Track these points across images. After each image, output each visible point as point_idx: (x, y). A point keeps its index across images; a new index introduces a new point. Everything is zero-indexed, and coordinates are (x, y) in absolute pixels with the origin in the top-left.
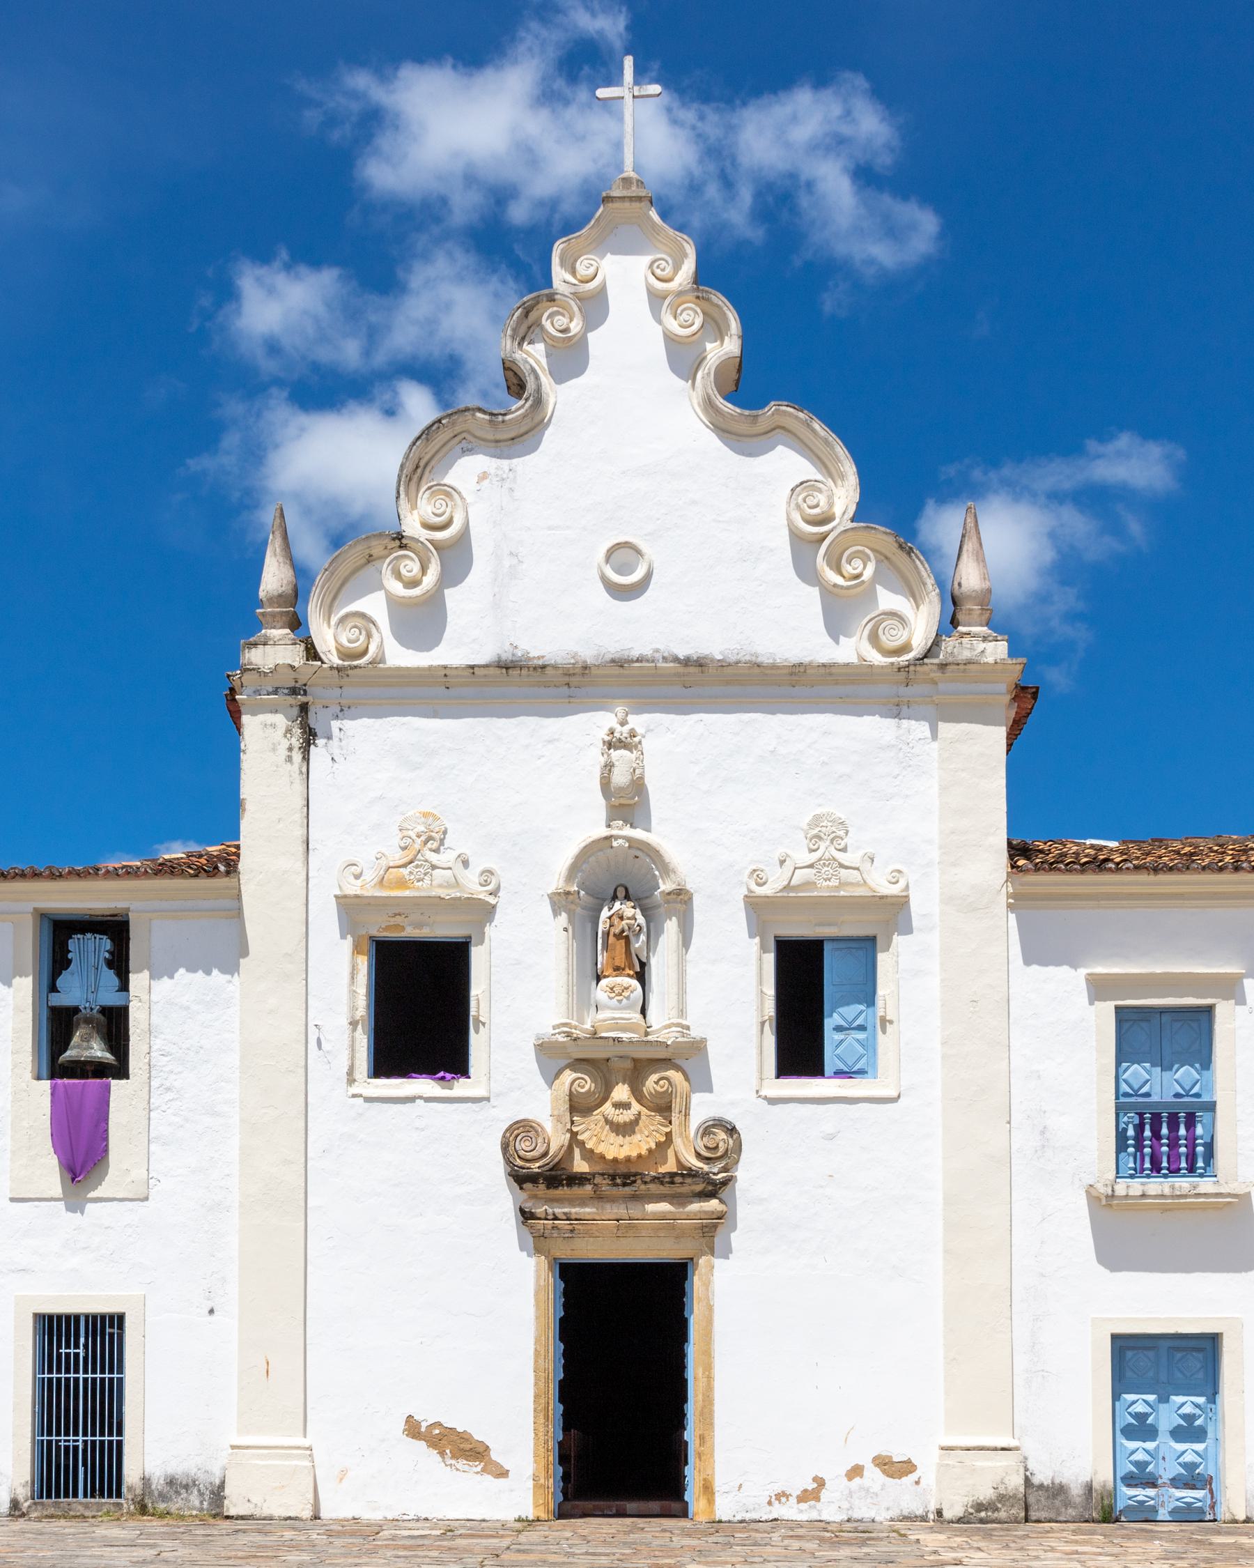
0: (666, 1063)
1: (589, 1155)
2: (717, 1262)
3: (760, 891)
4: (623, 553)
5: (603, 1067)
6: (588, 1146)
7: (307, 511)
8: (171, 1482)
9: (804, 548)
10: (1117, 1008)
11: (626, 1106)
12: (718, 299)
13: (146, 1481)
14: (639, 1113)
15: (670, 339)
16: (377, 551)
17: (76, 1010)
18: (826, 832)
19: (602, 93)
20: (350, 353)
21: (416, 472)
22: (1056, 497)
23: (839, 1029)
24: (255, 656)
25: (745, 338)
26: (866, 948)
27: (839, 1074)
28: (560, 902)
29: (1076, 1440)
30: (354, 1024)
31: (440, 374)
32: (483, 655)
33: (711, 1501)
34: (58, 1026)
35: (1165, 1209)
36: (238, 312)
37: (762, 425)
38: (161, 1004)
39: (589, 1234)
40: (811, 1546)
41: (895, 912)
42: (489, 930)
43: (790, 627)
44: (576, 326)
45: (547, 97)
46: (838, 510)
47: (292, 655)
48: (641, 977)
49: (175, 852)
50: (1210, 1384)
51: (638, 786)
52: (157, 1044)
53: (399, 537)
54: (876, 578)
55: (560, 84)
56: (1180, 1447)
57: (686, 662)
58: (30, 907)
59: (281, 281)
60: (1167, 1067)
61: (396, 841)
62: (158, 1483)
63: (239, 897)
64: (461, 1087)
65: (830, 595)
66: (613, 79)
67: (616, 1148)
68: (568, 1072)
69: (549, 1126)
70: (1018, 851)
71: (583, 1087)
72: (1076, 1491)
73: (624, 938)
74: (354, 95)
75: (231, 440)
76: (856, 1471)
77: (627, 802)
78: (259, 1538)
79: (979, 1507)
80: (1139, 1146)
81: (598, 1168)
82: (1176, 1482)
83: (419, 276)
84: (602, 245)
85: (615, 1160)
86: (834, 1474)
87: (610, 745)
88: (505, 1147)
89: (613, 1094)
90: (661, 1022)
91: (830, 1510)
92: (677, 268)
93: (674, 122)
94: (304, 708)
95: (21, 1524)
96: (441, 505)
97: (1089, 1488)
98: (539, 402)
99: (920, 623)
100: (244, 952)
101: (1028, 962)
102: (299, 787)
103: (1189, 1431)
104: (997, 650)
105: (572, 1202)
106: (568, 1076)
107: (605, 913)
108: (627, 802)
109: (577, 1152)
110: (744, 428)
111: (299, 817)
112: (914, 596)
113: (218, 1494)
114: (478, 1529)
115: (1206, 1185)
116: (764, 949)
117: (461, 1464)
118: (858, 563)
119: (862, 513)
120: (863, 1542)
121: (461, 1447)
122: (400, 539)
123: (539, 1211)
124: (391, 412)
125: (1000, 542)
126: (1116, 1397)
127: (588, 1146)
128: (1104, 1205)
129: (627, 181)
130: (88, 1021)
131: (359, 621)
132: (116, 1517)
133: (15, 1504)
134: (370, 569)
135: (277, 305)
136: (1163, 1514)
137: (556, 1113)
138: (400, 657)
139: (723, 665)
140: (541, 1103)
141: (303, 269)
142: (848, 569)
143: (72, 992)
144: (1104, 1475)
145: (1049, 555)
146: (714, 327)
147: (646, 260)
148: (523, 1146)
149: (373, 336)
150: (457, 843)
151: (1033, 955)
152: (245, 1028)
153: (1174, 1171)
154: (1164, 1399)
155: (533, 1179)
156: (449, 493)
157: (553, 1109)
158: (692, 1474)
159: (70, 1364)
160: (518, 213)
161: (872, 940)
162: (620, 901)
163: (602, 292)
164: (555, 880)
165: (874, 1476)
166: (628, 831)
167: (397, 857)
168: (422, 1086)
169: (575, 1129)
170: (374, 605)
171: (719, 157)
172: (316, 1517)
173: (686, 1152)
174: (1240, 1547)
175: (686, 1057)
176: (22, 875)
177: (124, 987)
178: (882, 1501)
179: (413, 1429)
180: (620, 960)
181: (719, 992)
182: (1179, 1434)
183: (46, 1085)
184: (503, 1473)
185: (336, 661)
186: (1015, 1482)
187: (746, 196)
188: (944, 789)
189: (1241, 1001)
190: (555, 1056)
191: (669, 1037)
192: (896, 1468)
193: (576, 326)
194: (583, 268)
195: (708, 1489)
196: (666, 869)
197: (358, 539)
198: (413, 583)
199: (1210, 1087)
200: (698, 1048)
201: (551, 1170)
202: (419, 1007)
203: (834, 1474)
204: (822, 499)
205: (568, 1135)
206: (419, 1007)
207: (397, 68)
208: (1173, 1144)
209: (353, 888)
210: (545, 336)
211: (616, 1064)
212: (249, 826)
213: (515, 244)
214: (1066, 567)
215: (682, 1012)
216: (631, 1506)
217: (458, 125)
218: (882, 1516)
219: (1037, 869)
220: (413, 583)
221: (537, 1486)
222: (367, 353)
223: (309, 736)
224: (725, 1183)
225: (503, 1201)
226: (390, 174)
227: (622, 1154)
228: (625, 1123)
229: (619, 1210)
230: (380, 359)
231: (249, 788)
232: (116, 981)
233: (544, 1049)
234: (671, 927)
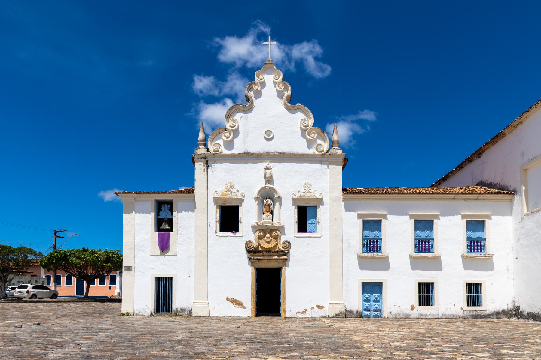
0: (277, 230)
1: (262, 247)
2: (286, 268)
4: (268, 132)
5: (264, 231)
7: (208, 123)
8: (182, 309)
9: (303, 131)
10: (363, 220)
11: (269, 238)
12: (287, 83)
13: (177, 309)
15: (278, 91)
16: (221, 131)
17: (163, 219)
18: (307, 186)
19: (265, 43)
20: (216, 93)
21: (228, 116)
22: (352, 122)
23: (310, 224)
24: (198, 151)
25: (292, 91)
26: (315, 208)
27: (310, 232)
28: (256, 199)
29: (354, 301)
30: (217, 222)
31: (234, 97)
33: (285, 313)
34: (159, 222)
35: (372, 258)
36: (194, 84)
37: (295, 108)
38: (180, 218)
39: (261, 262)
40: (304, 322)
41: (320, 201)
42: (242, 204)
43: (300, 146)
44: (259, 88)
45: (254, 44)
46: (310, 124)
47: (205, 151)
48: (272, 213)
49: (182, 189)
50: (380, 292)
51: (271, 177)
52: (179, 225)
53: (225, 129)
54: (317, 137)
55: (257, 41)
56: (375, 304)
57: (281, 153)
58: (154, 199)
59: (202, 78)
60: (372, 231)
61: (225, 187)
62: (179, 310)
63: (194, 197)
64: (237, 234)
65: (308, 140)
66: (266, 40)
67: (267, 246)
69: (254, 242)
70: (344, 190)
72: (355, 312)
73: (269, 206)
74: (217, 43)
75: (193, 110)
76: (313, 308)
77: (269, 180)
78: (198, 320)
79: (336, 315)
80: (367, 246)
82: (374, 310)
83: (229, 78)
84: (264, 73)
86: (309, 308)
87: (266, 169)
88: (246, 246)
90: (276, 222)
91: (308, 315)
92: (279, 77)
93: (279, 48)
94: (207, 161)
95: (153, 317)
96: (233, 122)
97: (357, 311)
98: (252, 103)
99: (325, 146)
100: (195, 208)
101: (346, 211)
102: (206, 176)
103: (376, 301)
104: (340, 152)
105: (259, 256)
106: (258, 232)
107: (265, 201)
108: (269, 180)
110: (292, 108)
111: (206, 182)
112: (324, 141)
113: (190, 312)
114: (240, 318)
115: (380, 254)
116: (295, 208)
117: (237, 306)
118: (314, 134)
119: (314, 125)
120: (314, 321)
121: (237, 303)
122: (225, 129)
123: (252, 258)
124: (224, 104)
125: (341, 131)
126: (362, 294)
128: (360, 258)
129: (269, 60)
130: (165, 221)
131: (218, 145)
132: (171, 316)
133: (151, 313)
134: (220, 135)
135: (202, 84)
136: (371, 316)
138: (225, 152)
139: (288, 154)
140: (252, 237)
141: (207, 77)
142: (312, 136)
143: (162, 215)
144: (360, 309)
145: (351, 133)
146: (286, 89)
147: (273, 76)
148: (249, 245)
149: (221, 90)
150: (236, 188)
151: (347, 210)
152: (195, 223)
153: (374, 251)
154: (372, 295)
155: (251, 252)
156: (235, 120)
158: (282, 308)
159: (162, 287)
160: (249, 66)
161: (316, 207)
162: (268, 199)
163: (264, 82)
164: (255, 195)
165: (316, 309)
166: (269, 185)
167: (225, 190)
168: (230, 234)
170: (220, 142)
171: (288, 56)
172: (209, 316)
173: (280, 247)
174: (386, 323)
175: (280, 229)
176: (153, 193)
177: (172, 214)
178: (318, 314)
179: (228, 299)
180: (268, 210)
181: (287, 216)
182: (374, 301)
183: (157, 233)
184: (245, 308)
185: (213, 152)
186: (343, 310)
187: (293, 64)
188: (330, 178)
189: (387, 219)
190: (255, 228)
191: (277, 225)
192: (320, 307)
193: (259, 88)
194: (261, 77)
195: (284, 311)
196: (277, 193)
197: (218, 128)
198: (228, 138)
199: (381, 235)
200: (283, 227)
202: (229, 219)
203: (309, 308)
204: (307, 122)
206: (229, 219)
207: (225, 38)
208: (374, 246)
209: (216, 196)
210: (253, 90)
211: (267, 230)
212: (196, 184)
213: (248, 72)
214: (355, 136)
215: (280, 220)
216: (270, 314)
217: (237, 49)
218: (318, 317)
219: (348, 193)
220: (228, 138)
221: (252, 310)
222: (220, 93)
223: (208, 167)
224: (288, 253)
225: (245, 256)
226: (223, 58)
229: (268, 258)
230: (222, 94)
231: (196, 177)
233: (253, 227)
234: (278, 204)
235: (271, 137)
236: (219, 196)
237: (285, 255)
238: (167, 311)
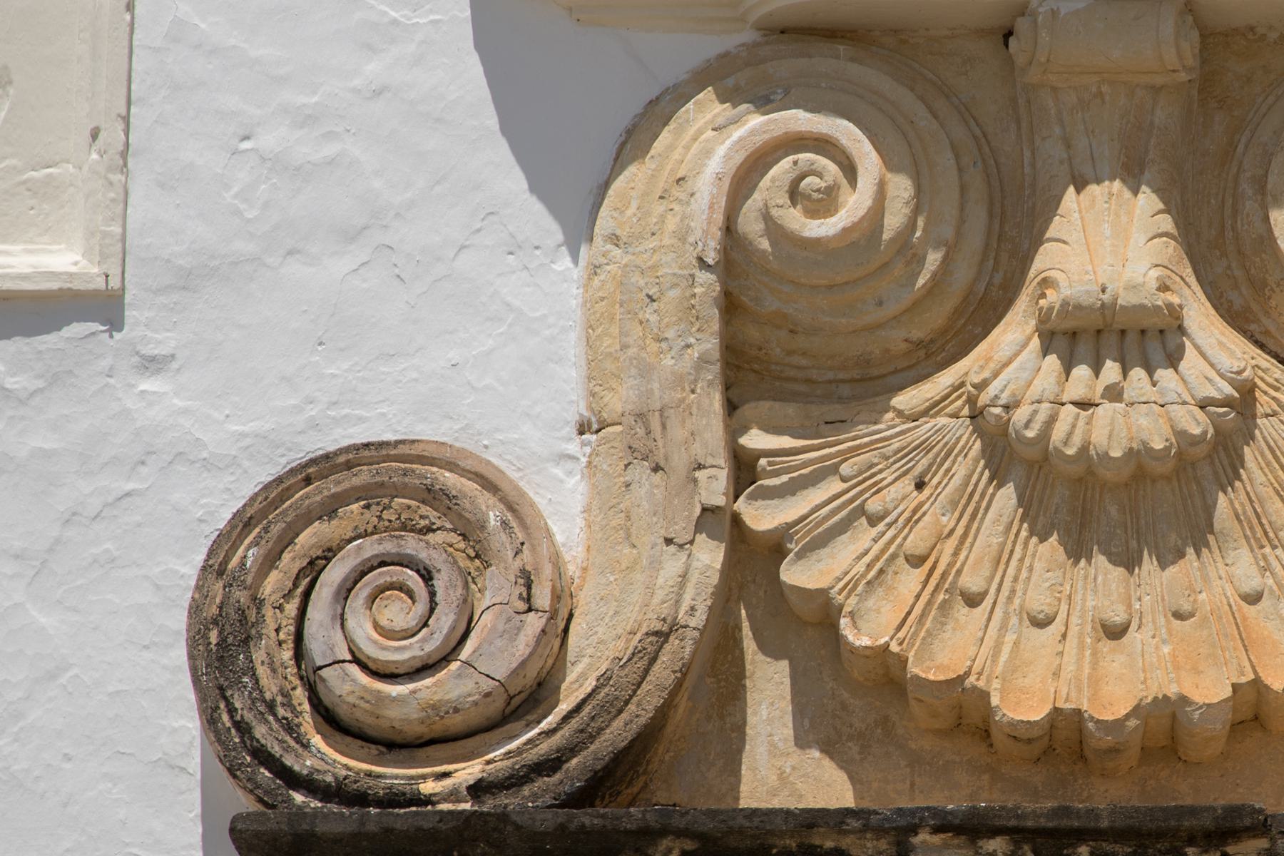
1: (859, 697)
6: (863, 633)
14: (1244, 400)
68: (705, 109)
69: (563, 503)
71: (824, 204)
85: (1065, 740)
89: (1045, 260)
106: (711, 140)
109: (769, 691)
127: (858, 636)
137: (618, 401)
157: (597, 373)
169: (763, 517)
201: (585, 796)
205: (710, 556)
227: (1113, 691)
228: (1139, 457)
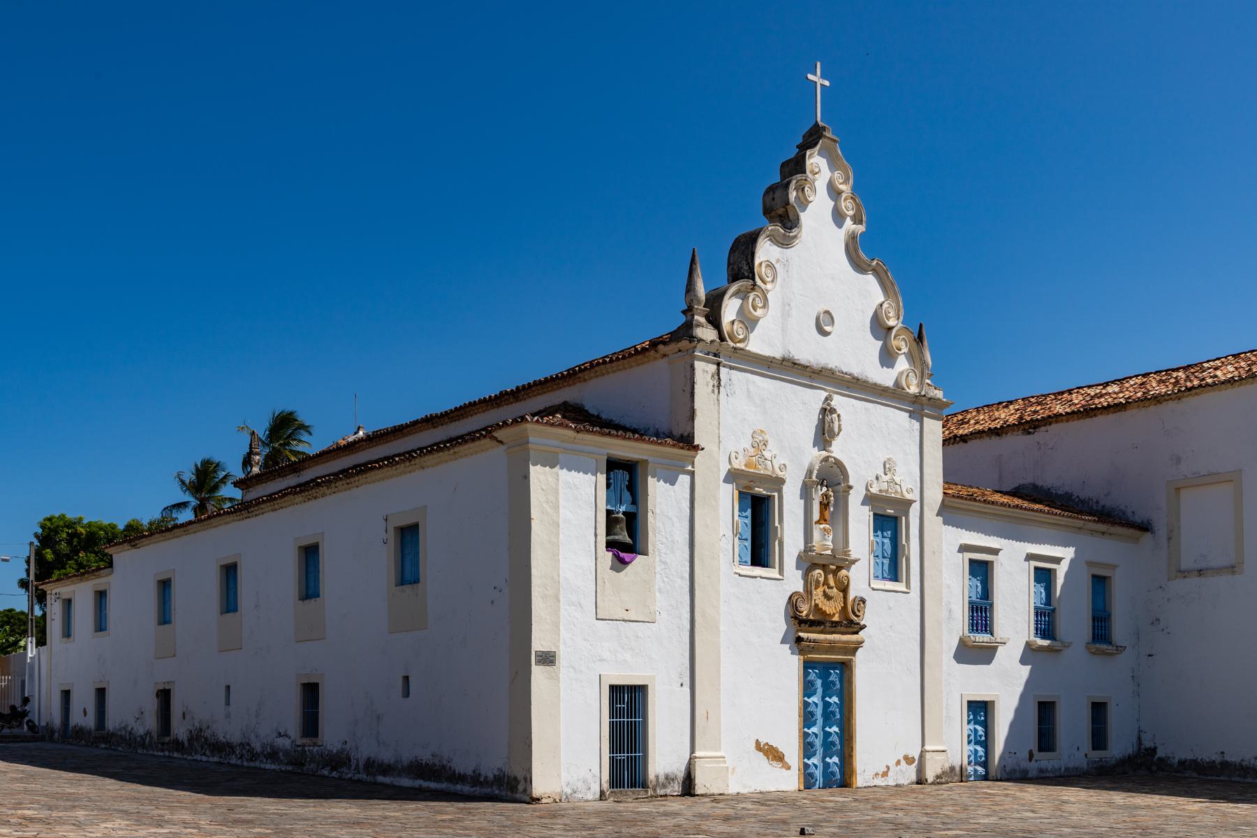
3: (874, 490)
8: (667, 777)
13: (657, 777)
32: (778, 355)
53: (755, 285)
62: (662, 779)
72: (958, 769)
76: (898, 763)
79: (938, 777)
81: (818, 618)
86: (892, 764)
117: (774, 763)
121: (773, 754)
133: (602, 793)
165: (903, 762)
179: (759, 747)
184: (789, 768)
231: (699, 403)
232: (630, 499)
235: (827, 329)
236: (739, 464)
237: (857, 633)
238: (633, 785)
